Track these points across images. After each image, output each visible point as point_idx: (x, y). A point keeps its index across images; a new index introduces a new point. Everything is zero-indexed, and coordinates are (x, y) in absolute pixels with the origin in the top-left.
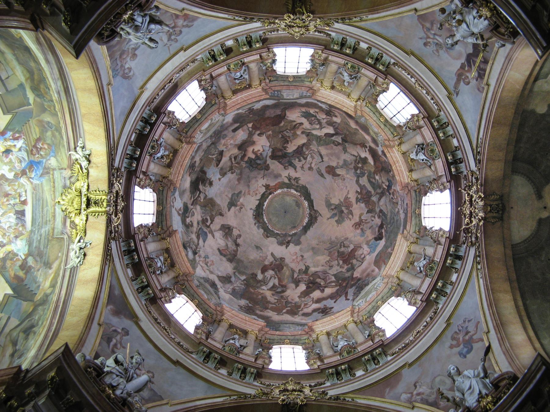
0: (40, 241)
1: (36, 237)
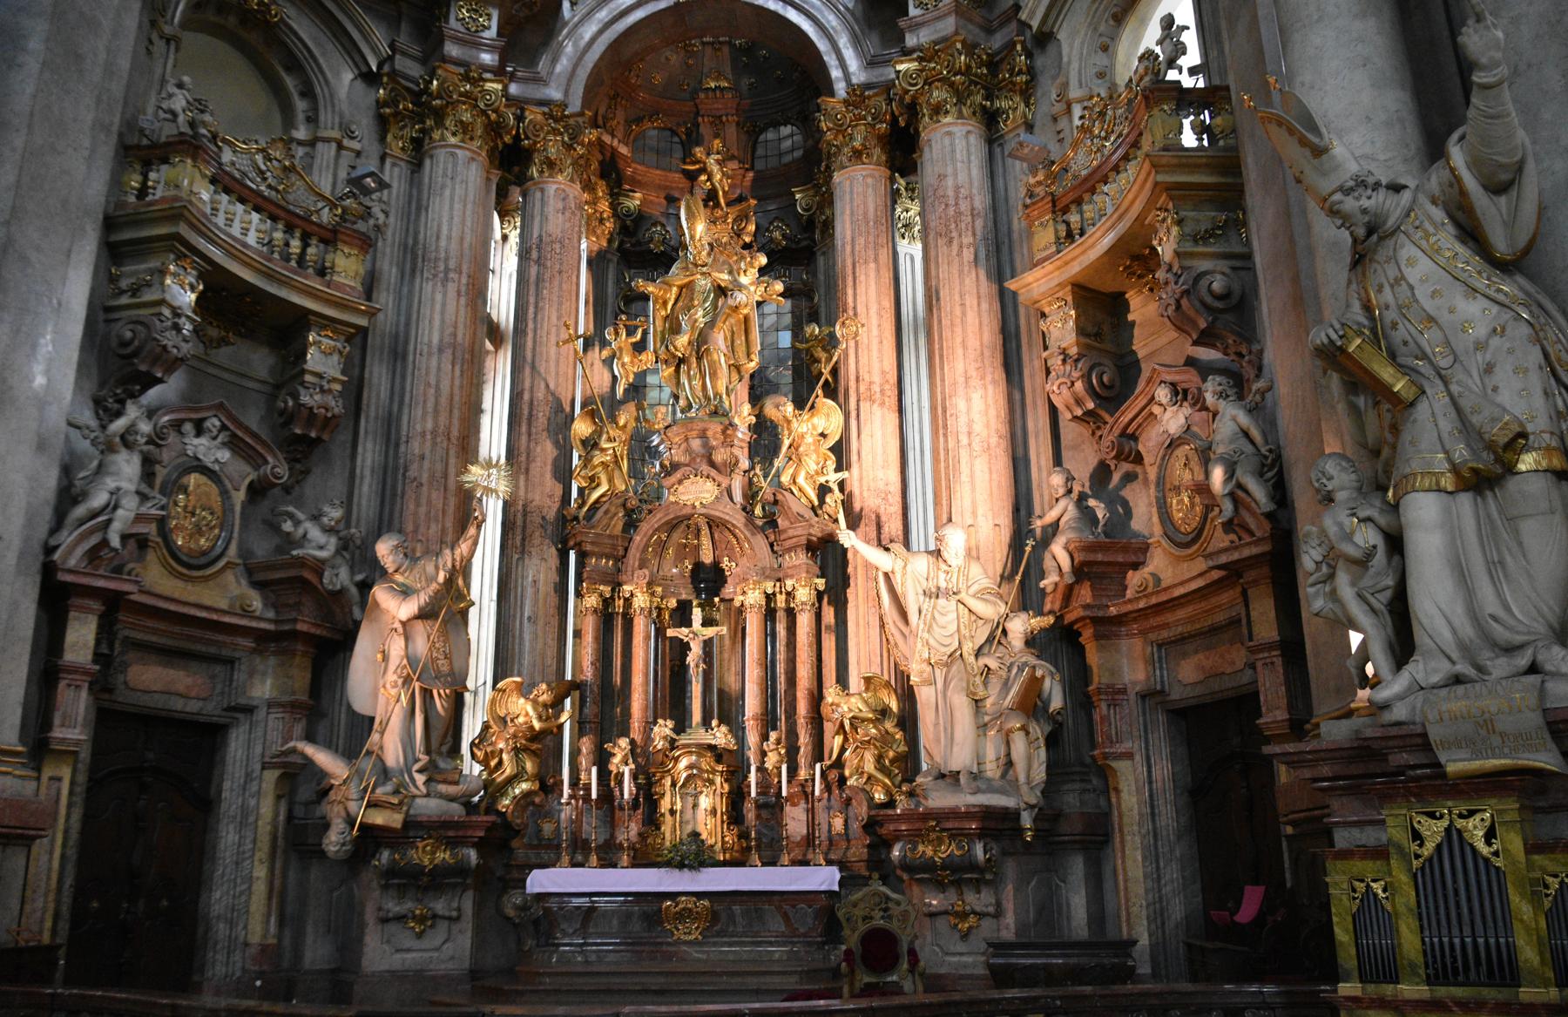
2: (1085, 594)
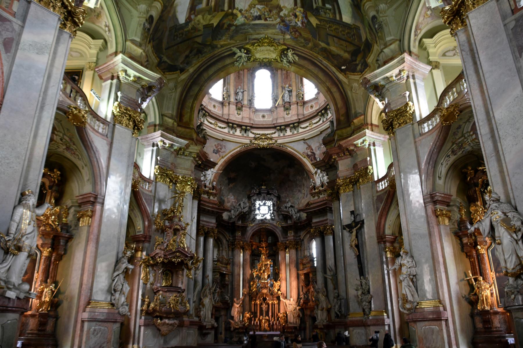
0: (244, 29)
1: (246, 27)
2: (304, 305)
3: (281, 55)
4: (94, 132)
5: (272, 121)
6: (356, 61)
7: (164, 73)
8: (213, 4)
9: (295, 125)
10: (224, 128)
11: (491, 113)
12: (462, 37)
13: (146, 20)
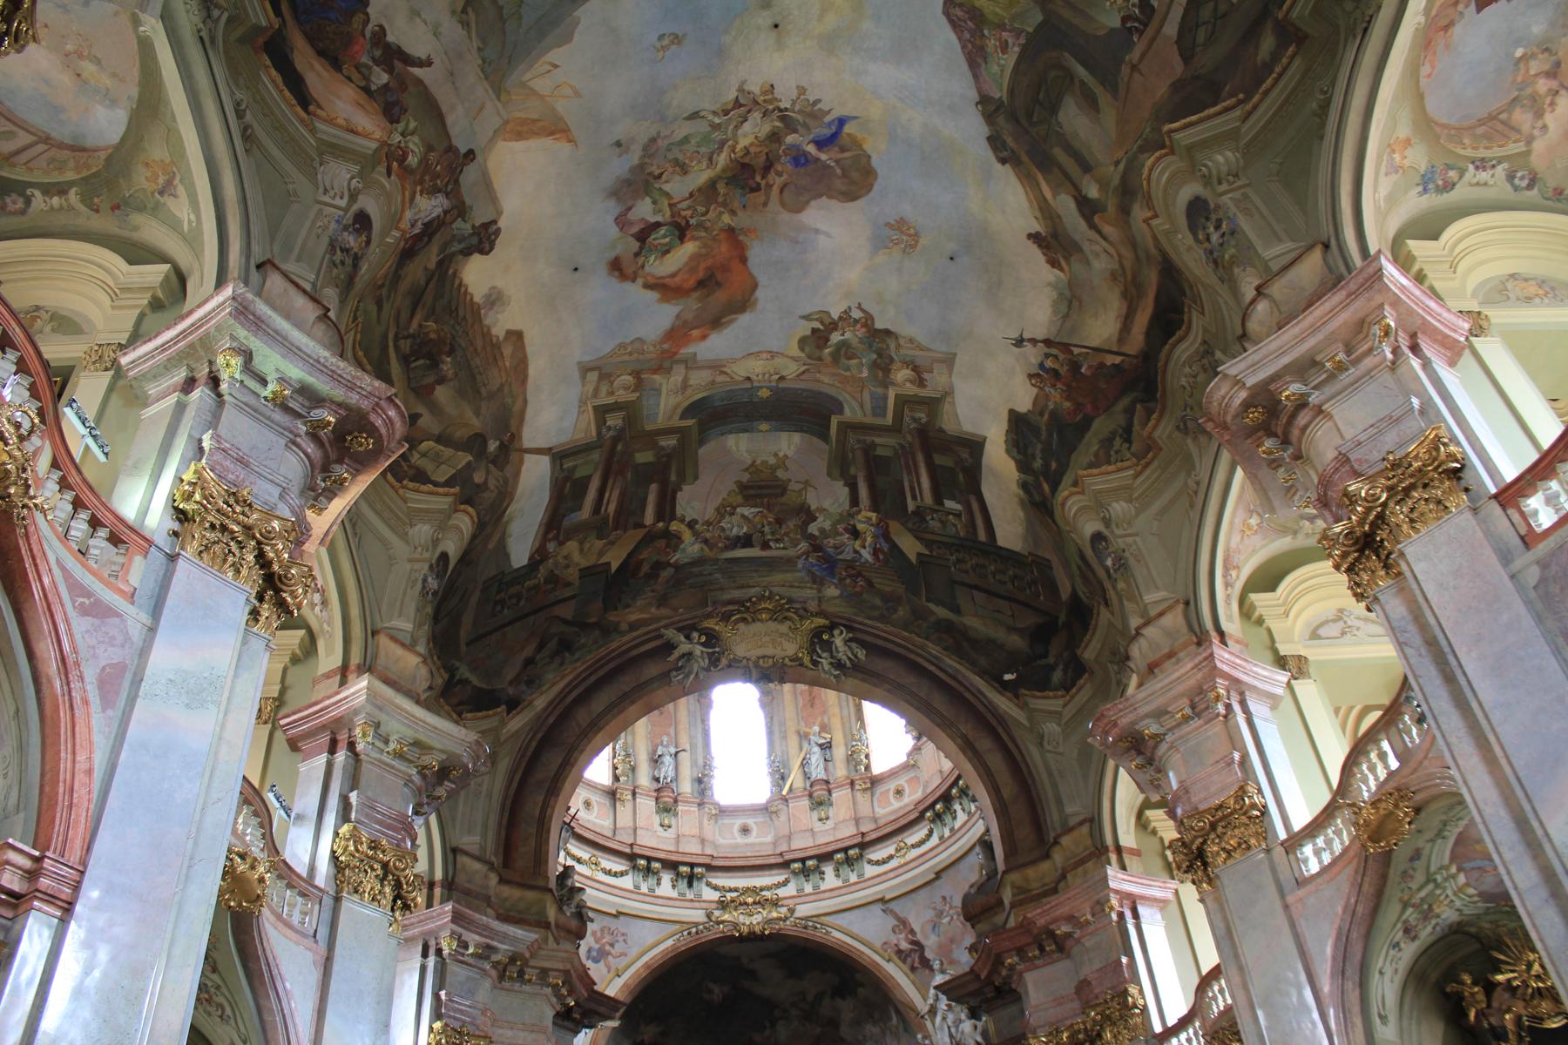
3: (812, 643)
4: (280, 925)
5: (775, 844)
6: (1045, 656)
7: (460, 715)
8: (612, 508)
9: (850, 854)
10: (622, 874)
11: (1535, 824)
12: (1396, 606)
13: (431, 567)
